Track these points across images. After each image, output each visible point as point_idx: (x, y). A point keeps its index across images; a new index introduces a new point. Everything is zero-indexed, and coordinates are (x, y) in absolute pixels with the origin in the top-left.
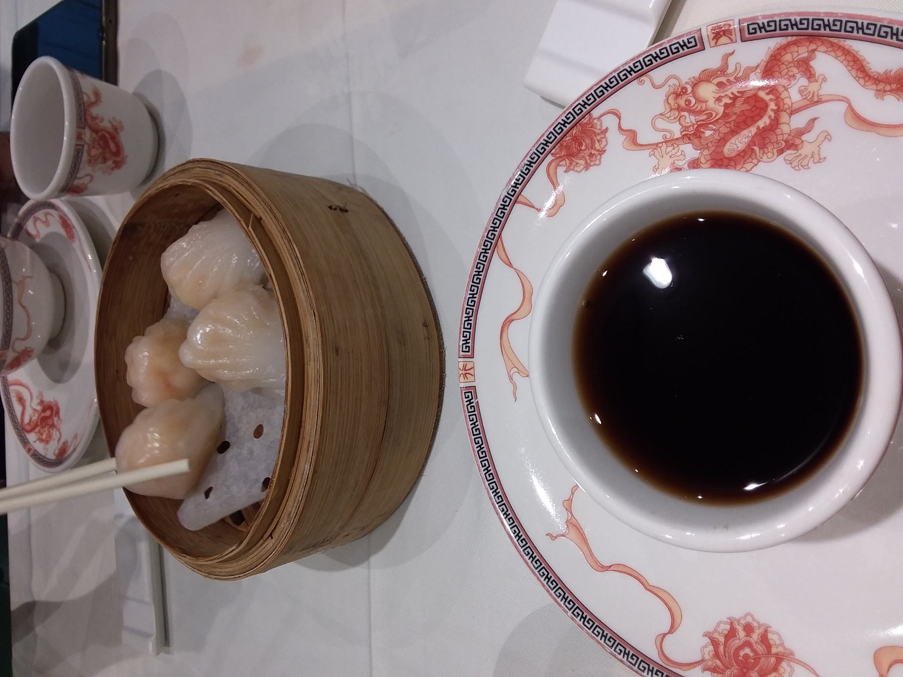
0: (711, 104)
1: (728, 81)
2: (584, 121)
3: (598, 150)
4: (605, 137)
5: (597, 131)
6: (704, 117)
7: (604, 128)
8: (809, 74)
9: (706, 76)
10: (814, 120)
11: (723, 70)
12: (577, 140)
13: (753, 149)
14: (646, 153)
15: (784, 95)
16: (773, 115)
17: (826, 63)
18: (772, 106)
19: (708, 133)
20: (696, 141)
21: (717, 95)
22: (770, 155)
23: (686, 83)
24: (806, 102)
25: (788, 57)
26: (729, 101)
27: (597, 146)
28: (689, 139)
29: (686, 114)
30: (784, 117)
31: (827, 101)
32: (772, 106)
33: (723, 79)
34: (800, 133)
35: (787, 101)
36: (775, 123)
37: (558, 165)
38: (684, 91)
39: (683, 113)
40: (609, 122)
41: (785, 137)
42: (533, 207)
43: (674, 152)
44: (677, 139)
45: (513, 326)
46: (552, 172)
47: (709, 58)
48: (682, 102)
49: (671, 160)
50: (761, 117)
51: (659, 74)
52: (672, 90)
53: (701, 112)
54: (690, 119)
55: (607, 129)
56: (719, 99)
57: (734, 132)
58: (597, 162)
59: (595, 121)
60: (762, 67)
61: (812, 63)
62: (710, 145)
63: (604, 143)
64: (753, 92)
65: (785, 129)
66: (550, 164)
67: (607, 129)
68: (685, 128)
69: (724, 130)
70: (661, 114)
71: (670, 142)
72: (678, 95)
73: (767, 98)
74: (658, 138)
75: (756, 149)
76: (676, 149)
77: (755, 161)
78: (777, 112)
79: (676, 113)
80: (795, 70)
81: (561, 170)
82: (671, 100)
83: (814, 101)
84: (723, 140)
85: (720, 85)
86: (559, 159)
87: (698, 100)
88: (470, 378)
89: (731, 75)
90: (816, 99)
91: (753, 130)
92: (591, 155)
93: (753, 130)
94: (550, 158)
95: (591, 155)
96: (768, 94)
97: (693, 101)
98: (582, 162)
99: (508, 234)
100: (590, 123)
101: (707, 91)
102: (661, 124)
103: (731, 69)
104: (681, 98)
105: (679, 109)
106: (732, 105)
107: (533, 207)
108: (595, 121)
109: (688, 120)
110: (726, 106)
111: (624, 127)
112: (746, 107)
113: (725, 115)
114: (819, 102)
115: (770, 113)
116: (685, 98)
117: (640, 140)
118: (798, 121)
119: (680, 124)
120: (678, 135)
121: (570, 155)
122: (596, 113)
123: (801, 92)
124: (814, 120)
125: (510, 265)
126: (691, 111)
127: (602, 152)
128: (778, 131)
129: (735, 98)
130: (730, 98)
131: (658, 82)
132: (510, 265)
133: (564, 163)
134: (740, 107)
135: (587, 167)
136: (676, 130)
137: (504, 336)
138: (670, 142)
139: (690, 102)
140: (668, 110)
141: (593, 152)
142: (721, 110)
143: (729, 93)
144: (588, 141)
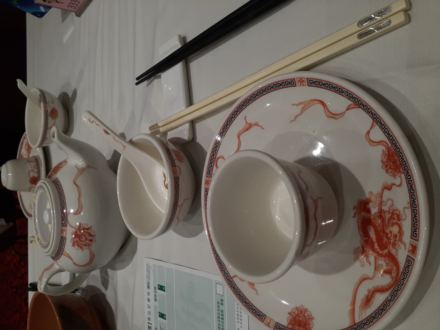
0: (391, 229)
1: (396, 241)
2: (401, 169)
3: (388, 170)
4: (392, 176)
5: (396, 173)
6: (386, 222)
7: (396, 177)
8: (386, 272)
9: (401, 232)
10: (370, 264)
11: (401, 240)
12: (394, 162)
13: (366, 237)
14: (380, 191)
15: (383, 258)
16: (378, 250)
17: (387, 280)
18: (381, 252)
19: (380, 221)
20: (378, 215)
21: (393, 232)
22: (363, 243)
23: (402, 222)
24: (377, 265)
25: (395, 268)
26: (389, 236)
27: (390, 170)
28: (380, 212)
29: (390, 215)
30: (375, 254)
31: (374, 273)
32: (381, 252)
33: (398, 238)
34: (367, 256)
35: (380, 258)
36: (374, 250)
37: (386, 148)
38: (399, 219)
39: (391, 214)
40: (397, 181)
41: (368, 251)
42: (371, 129)
43: (376, 204)
44: (381, 207)
45: (321, 107)
46: (384, 143)
47: (407, 237)
48: (395, 216)
49: (373, 201)
50: (378, 246)
51: (409, 212)
52: (401, 215)
53: (389, 222)
54: (387, 216)
55: (395, 178)
56: (391, 232)
57: (376, 232)
58: (383, 167)
59: (400, 174)
60: (396, 256)
61: (389, 275)
62: (375, 220)
63: (390, 174)
64: (389, 247)
65: (371, 252)
66: (387, 144)
67: (395, 178)
68: (385, 212)
69: (379, 228)
70: (393, 204)
71: (381, 203)
72: (398, 216)
73: (384, 252)
74: (384, 199)
75: (367, 238)
76: (377, 205)
77: (362, 236)
78: (378, 253)
79: (391, 211)
80: (390, 268)
81: (384, 148)
82: (398, 213)
83: (377, 268)
84: (375, 227)
85: (396, 236)
86: (389, 149)
87: (393, 224)
88: (303, 79)
89: (398, 242)
90: (377, 269)
91: (374, 240)
92: (387, 166)
93: (374, 240)
94: (390, 145)
95: (387, 166)
96: (386, 253)
97: (394, 221)
98: (385, 160)
99: (360, 112)
100: (399, 172)
101: (395, 230)
102: (389, 203)
103: (400, 243)
104: (396, 217)
105: (393, 214)
106: (387, 237)
107: (371, 129)
108: (400, 174)
109: (387, 215)
110: (387, 234)
111: (394, 187)
112: (384, 241)
113: (384, 232)
114: (375, 269)
115: (378, 250)
116: (396, 218)
117: (386, 191)
118: (372, 258)
119: (387, 211)
120: (383, 208)
121: (389, 156)
122: (403, 176)
123: (382, 265)
124: (370, 264)
125: (348, 109)
126: (391, 218)
127: (387, 172)
128: (371, 250)
129: (389, 239)
130: (390, 237)
131: (406, 210)
132: (348, 109)
133: (387, 151)
134: (385, 240)
135: (382, 161)
136: (385, 208)
137: (317, 102)
138: (381, 203)
139: (394, 220)
140: (394, 209)
141: (388, 167)
142: (387, 231)
143: (392, 238)
144: (392, 167)
